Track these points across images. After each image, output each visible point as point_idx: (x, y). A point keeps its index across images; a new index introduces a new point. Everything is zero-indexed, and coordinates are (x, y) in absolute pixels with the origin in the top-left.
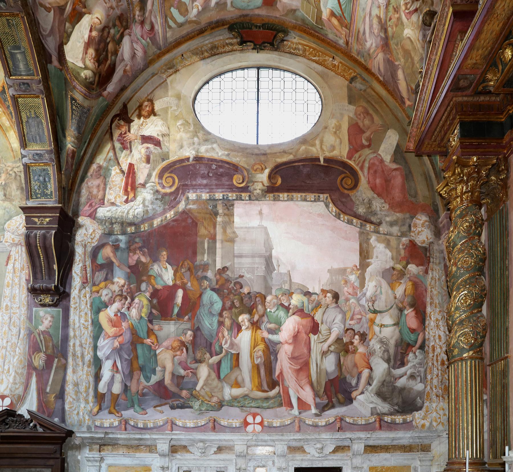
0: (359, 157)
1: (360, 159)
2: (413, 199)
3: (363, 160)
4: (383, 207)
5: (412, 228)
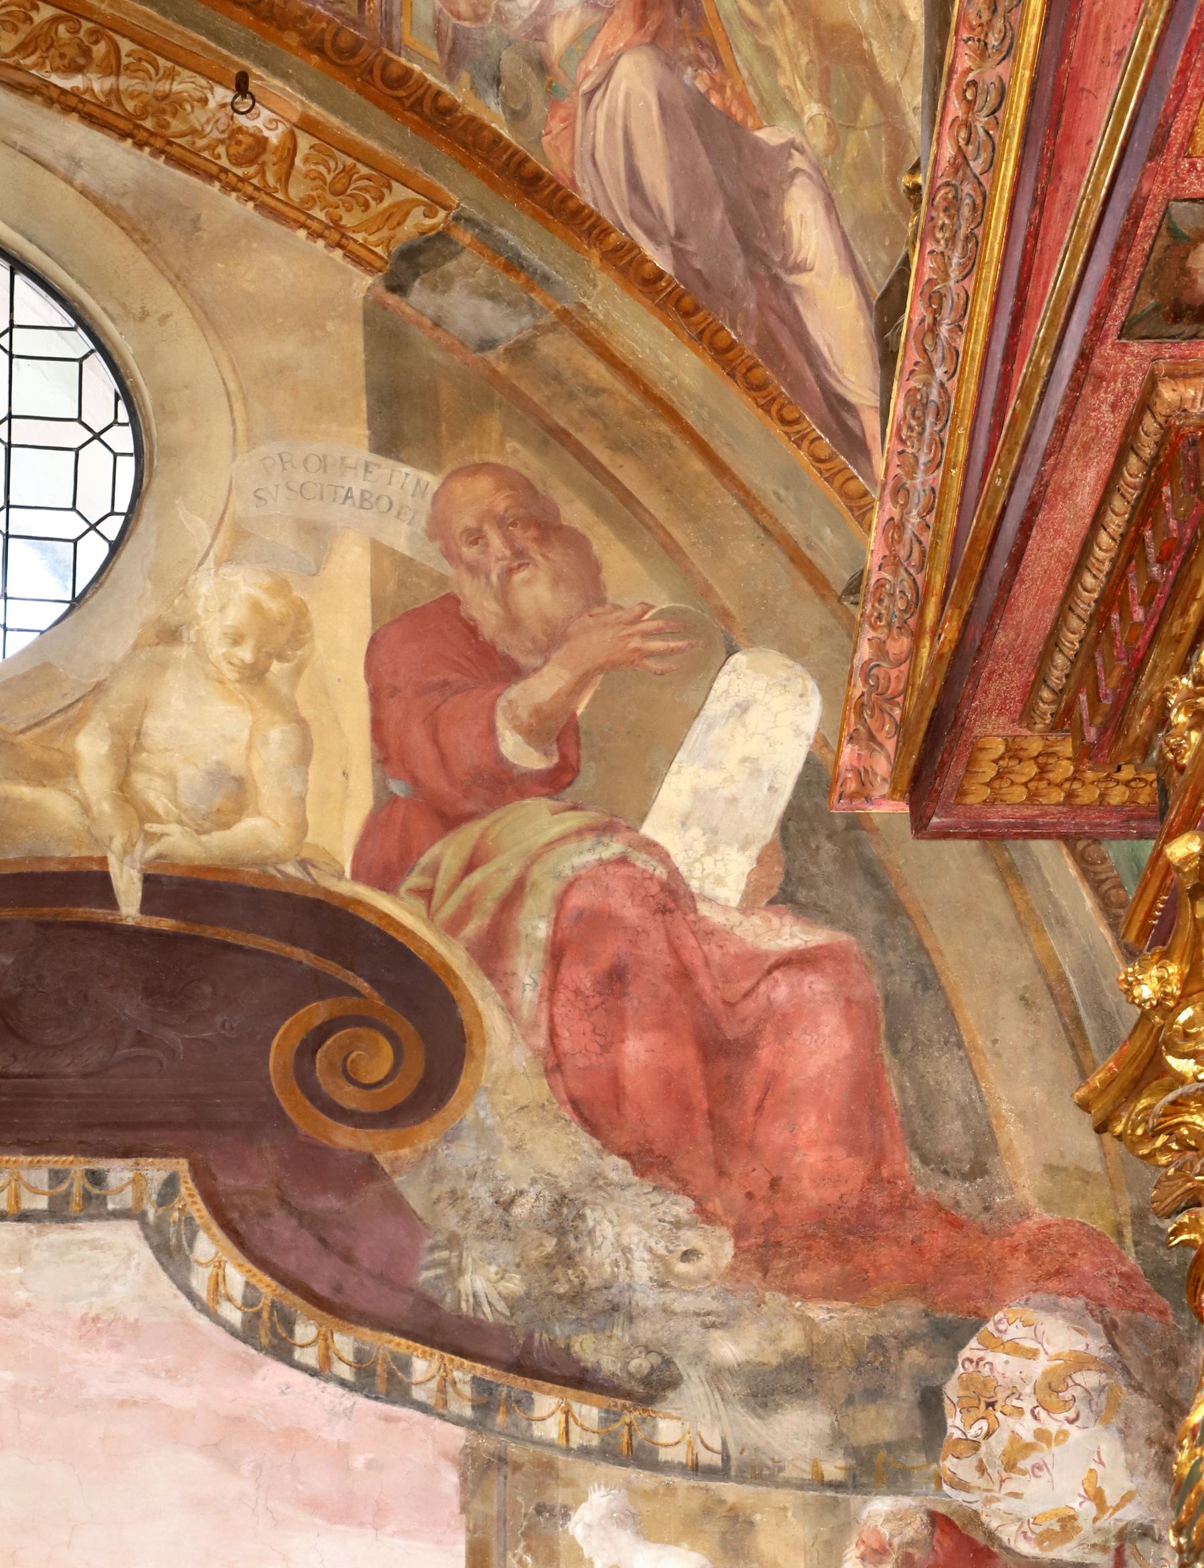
0: (470, 867)
1: (476, 877)
2: (956, 1191)
3: (502, 885)
5: (955, 1423)
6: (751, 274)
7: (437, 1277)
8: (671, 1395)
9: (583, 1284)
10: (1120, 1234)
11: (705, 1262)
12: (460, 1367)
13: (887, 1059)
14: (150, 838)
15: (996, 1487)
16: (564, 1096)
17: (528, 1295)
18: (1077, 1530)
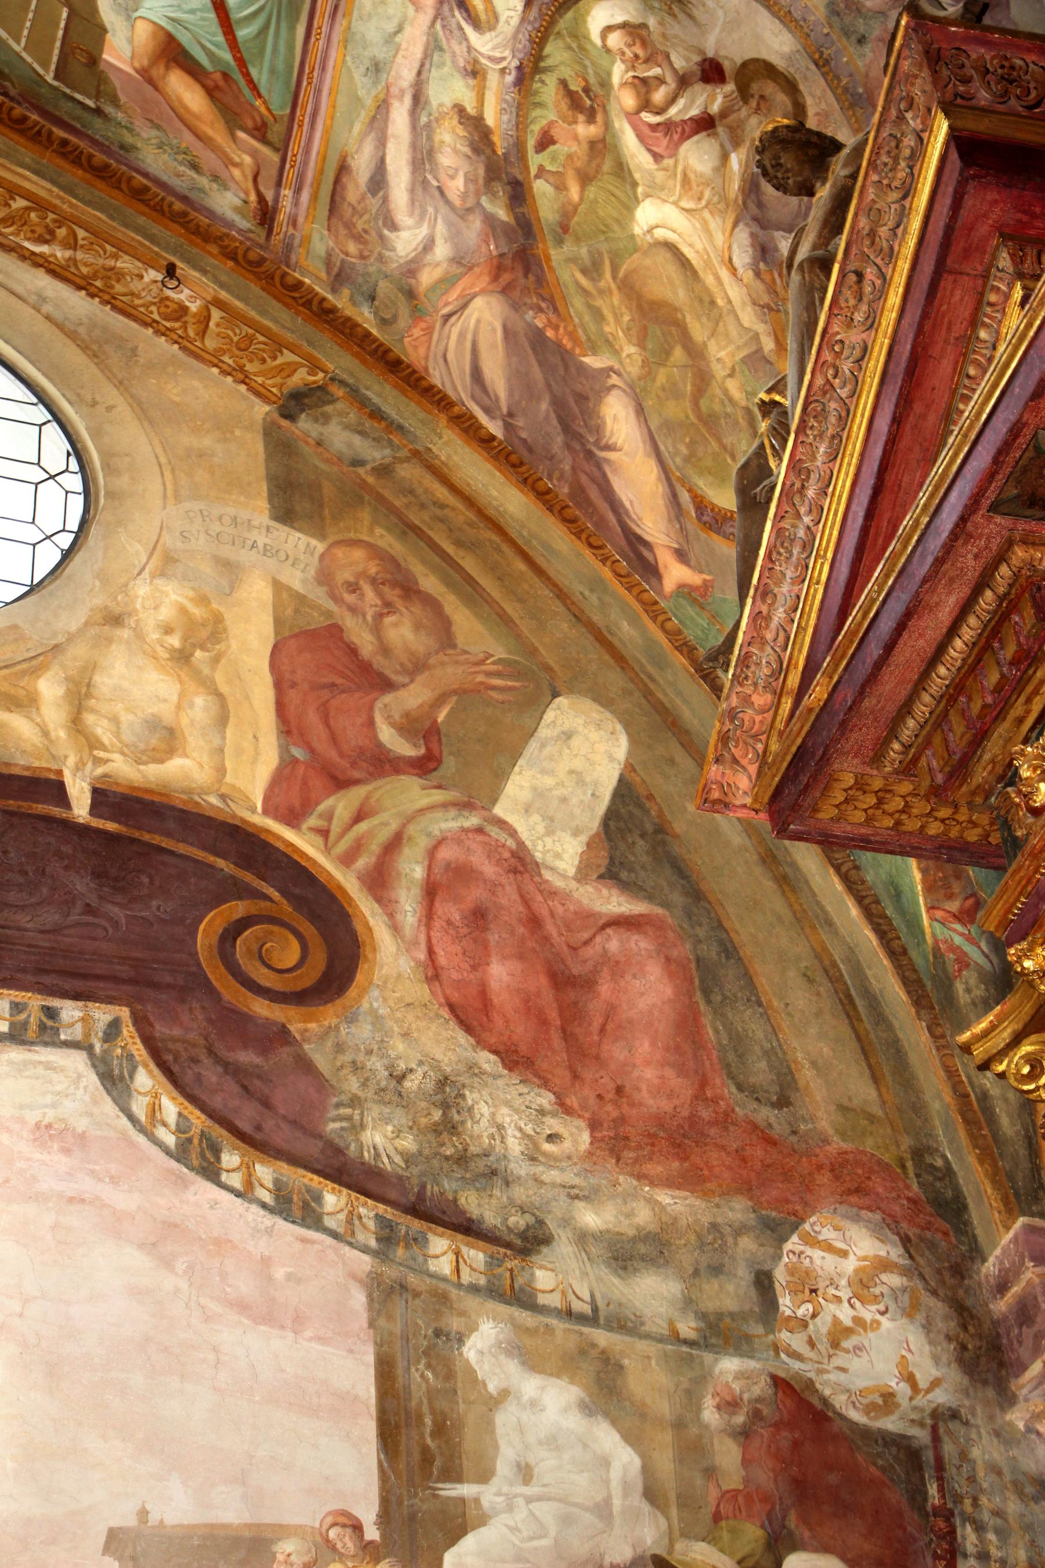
0: (359, 817)
1: (363, 826)
2: (765, 1114)
3: (384, 835)
4: (551, 1138)
5: (785, 1303)
7: (342, 1129)
8: (545, 1250)
9: (466, 1150)
10: (903, 1167)
11: (567, 1145)
12: (365, 1204)
13: (702, 1006)
14: (98, 761)
15: (826, 1361)
16: (442, 1000)
17: (420, 1153)
18: (898, 1405)
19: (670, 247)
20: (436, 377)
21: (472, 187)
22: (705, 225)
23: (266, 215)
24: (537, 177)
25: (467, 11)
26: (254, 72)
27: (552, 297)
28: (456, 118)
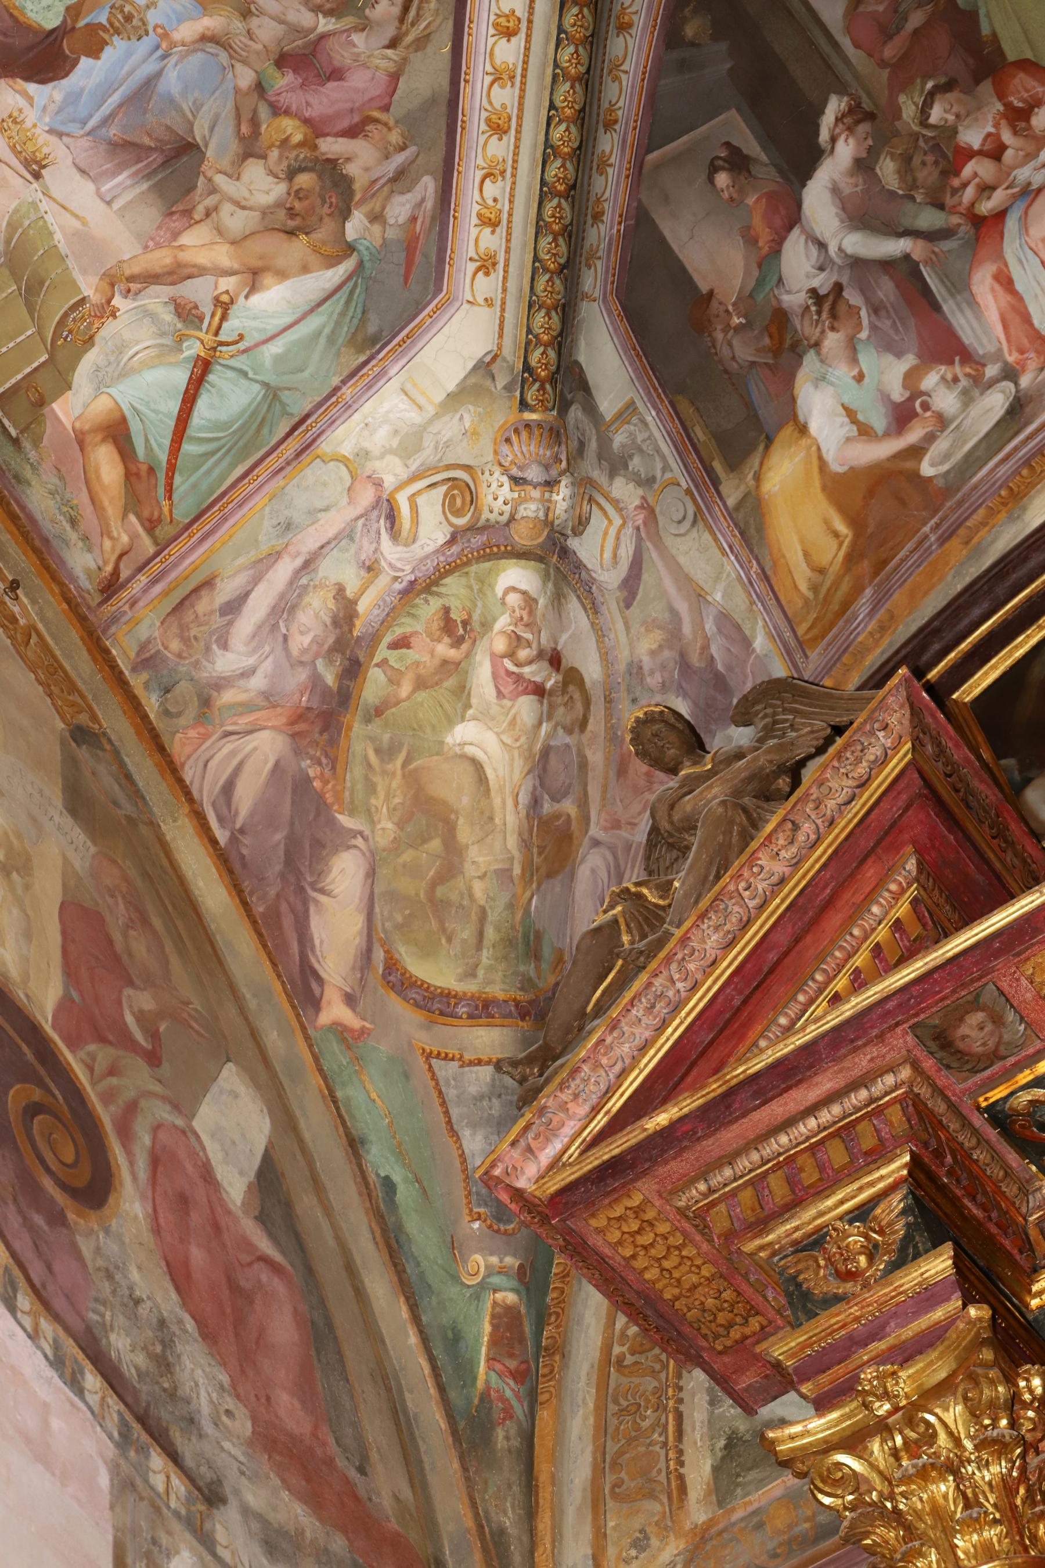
4: (228, 1412)
6: (282, 876)
19: (477, 765)
20: (188, 774)
21: (314, 648)
22: (512, 760)
23: (111, 587)
24: (377, 665)
25: (393, 524)
26: (178, 479)
27: (337, 758)
28: (334, 592)
